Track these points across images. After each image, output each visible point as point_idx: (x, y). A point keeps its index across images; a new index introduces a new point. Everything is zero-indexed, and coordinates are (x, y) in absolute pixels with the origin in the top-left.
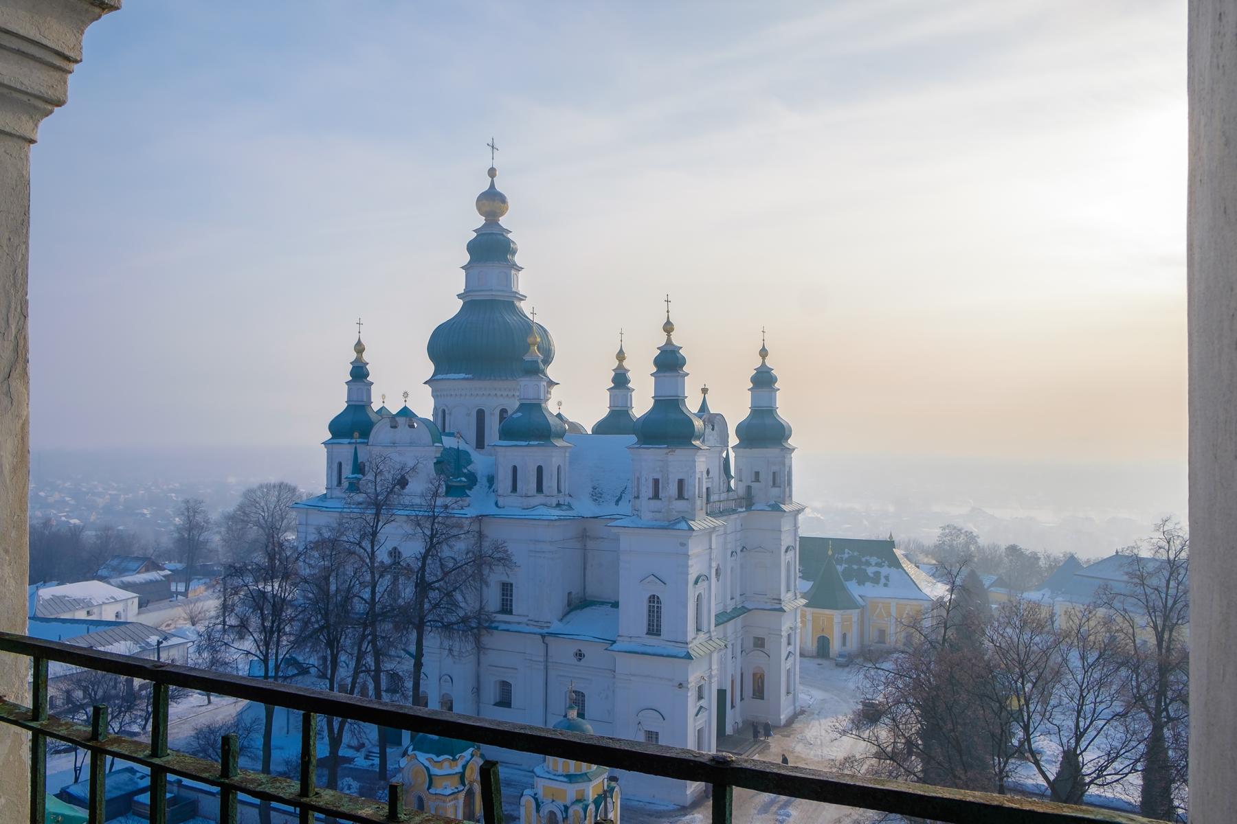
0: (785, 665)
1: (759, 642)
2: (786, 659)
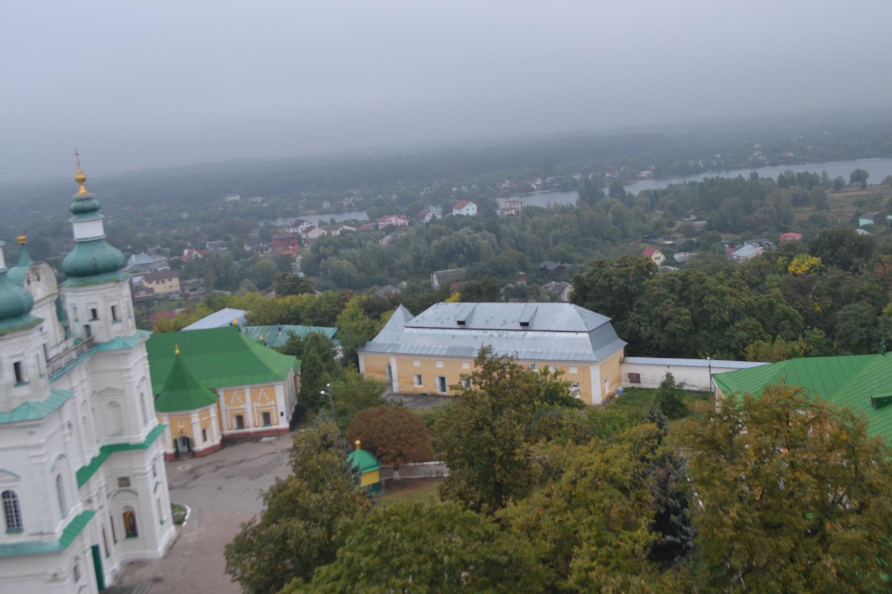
0: (153, 499)
1: (125, 482)
2: (155, 490)
